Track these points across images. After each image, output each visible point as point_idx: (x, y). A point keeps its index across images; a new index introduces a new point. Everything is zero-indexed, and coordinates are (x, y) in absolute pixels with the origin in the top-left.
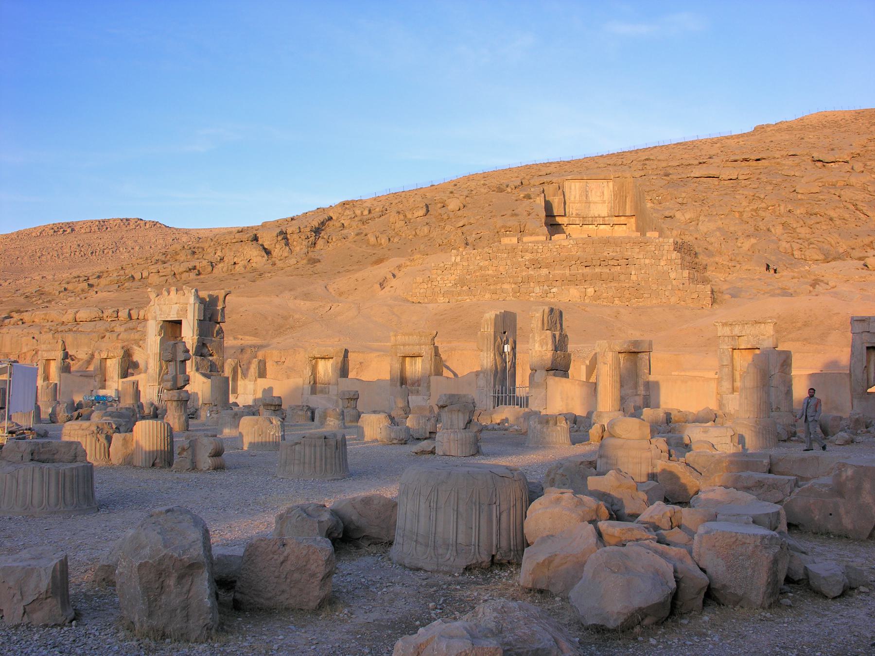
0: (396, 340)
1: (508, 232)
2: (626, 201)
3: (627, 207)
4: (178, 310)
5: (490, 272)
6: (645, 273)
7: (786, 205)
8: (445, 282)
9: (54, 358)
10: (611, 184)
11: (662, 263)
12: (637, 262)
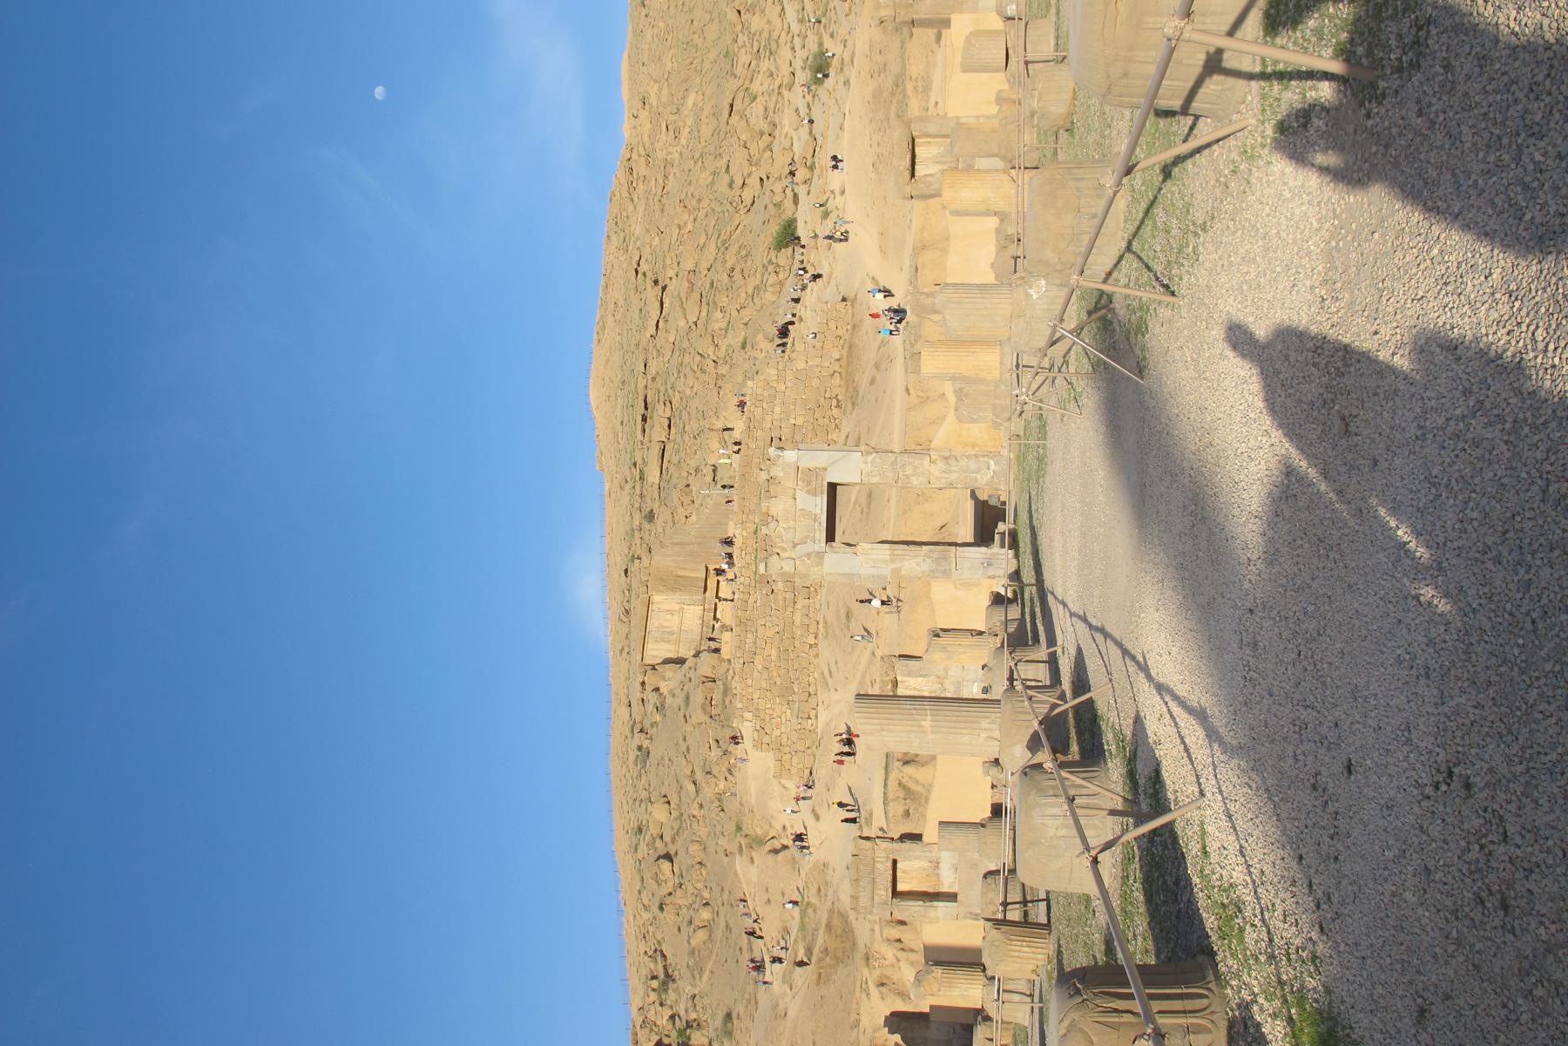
0: (887, 6)
2: (685, 577)
3: (692, 575)
4: (808, 492)
5: (774, 653)
6: (794, 404)
8: (784, 721)
9: (890, 864)
10: (656, 598)
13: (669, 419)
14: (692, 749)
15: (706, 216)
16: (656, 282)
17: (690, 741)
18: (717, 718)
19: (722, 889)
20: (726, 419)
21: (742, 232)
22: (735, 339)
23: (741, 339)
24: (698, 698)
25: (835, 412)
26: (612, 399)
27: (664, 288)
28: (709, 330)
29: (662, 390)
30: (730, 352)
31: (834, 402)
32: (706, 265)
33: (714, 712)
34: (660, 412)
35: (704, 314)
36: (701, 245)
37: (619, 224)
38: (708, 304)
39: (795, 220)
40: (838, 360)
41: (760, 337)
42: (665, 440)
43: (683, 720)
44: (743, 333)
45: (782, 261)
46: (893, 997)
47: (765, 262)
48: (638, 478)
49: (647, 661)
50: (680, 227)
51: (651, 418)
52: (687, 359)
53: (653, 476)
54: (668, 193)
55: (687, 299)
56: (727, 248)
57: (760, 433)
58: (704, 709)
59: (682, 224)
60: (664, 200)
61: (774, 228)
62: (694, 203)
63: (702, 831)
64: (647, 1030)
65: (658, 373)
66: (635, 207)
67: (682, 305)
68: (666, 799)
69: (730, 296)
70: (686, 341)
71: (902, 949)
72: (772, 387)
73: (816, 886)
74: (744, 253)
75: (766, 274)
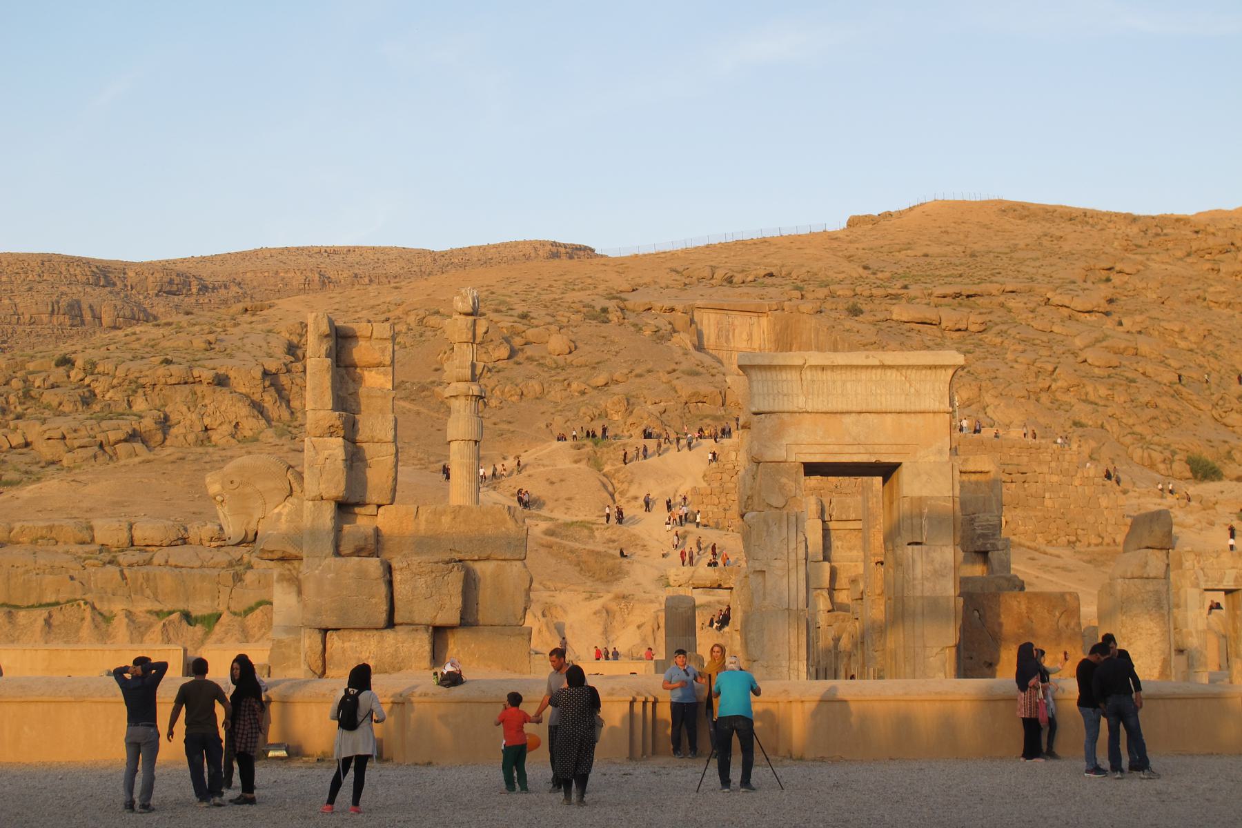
1: (700, 404)
6: (1065, 497)
7: (1095, 387)
10: (764, 321)
11: (1077, 483)
12: (1040, 478)
13: (966, 329)
14: (642, 380)
15: (1200, 366)
16: (1111, 301)
17: (650, 378)
18: (686, 410)
19: (510, 422)
20: (996, 407)
21: (1192, 413)
22: (1081, 412)
23: (1084, 421)
24: (704, 388)
25: (1064, 540)
26: (945, 238)
27: (1107, 314)
28: (1085, 381)
29: (993, 317)
30: (1068, 408)
31: (1073, 538)
32: (1150, 369)
33: (691, 406)
34: (973, 318)
35: (1096, 371)
36: (1166, 361)
37: (1158, 239)
38: (1109, 376)
39: (1220, 479)
40: (1114, 541)
41: (1093, 444)
42: (943, 325)
43: (670, 369)
44: (1090, 423)
45: (1176, 466)
46: (602, 623)
47: (1173, 447)
48: (890, 291)
49: (697, 315)
50: (1181, 332)
51: (960, 304)
52: (1044, 352)
53: (900, 312)
54: (1210, 308)
55: (1106, 347)
56: (1173, 396)
57: (1025, 459)
58: (694, 394)
59: (1185, 334)
60: (1199, 303)
61: (1208, 455)
62: (1210, 348)
63: (556, 393)
64: (299, 331)
65: (1010, 311)
66: (1181, 259)
67: (1097, 341)
68: (573, 349)
69: (1127, 405)
70: (1062, 349)
71: (653, 631)
72: (1077, 472)
73: (614, 537)
74: (1173, 418)
75: (1159, 449)
